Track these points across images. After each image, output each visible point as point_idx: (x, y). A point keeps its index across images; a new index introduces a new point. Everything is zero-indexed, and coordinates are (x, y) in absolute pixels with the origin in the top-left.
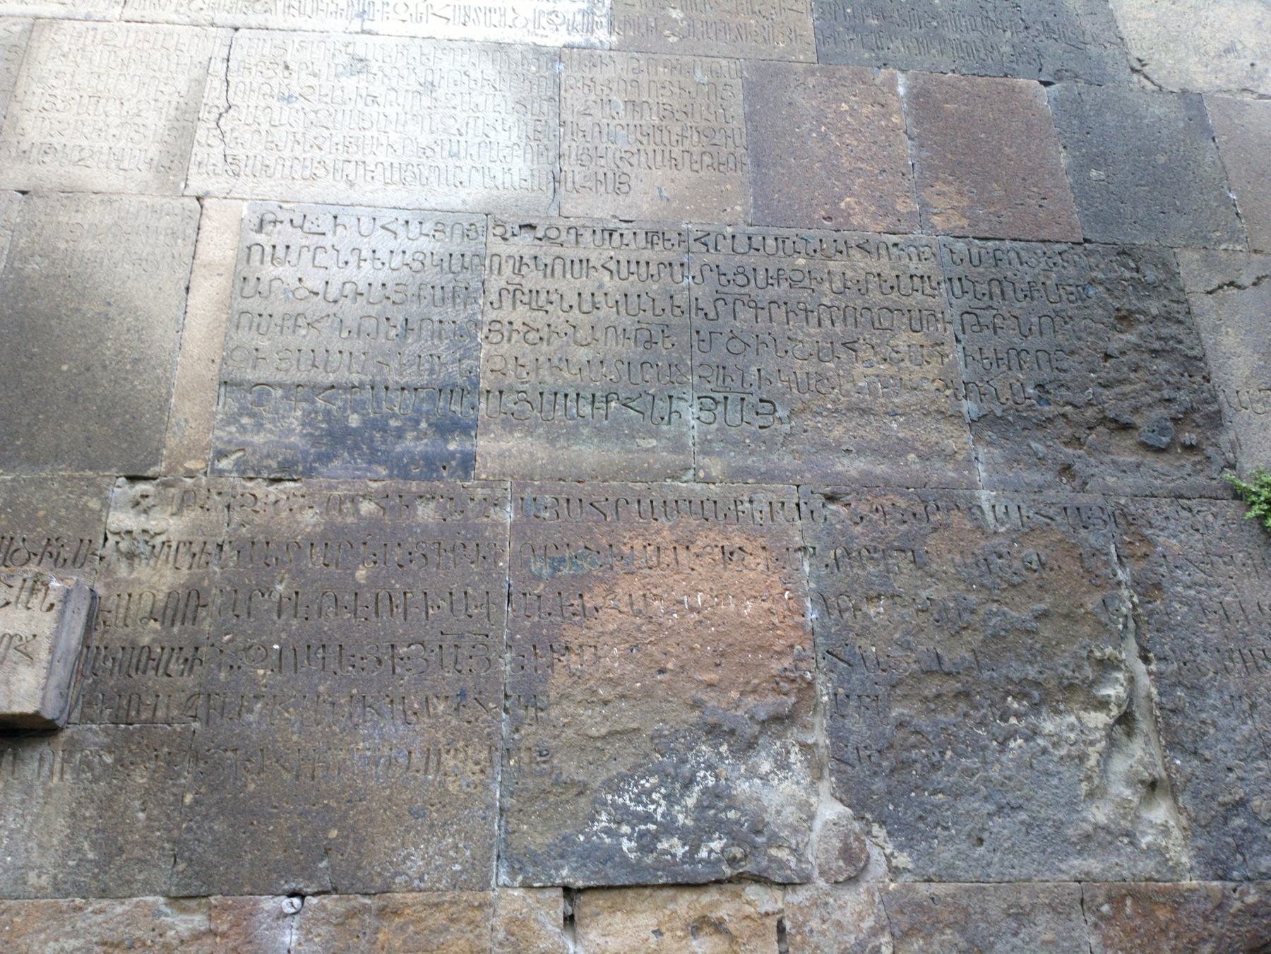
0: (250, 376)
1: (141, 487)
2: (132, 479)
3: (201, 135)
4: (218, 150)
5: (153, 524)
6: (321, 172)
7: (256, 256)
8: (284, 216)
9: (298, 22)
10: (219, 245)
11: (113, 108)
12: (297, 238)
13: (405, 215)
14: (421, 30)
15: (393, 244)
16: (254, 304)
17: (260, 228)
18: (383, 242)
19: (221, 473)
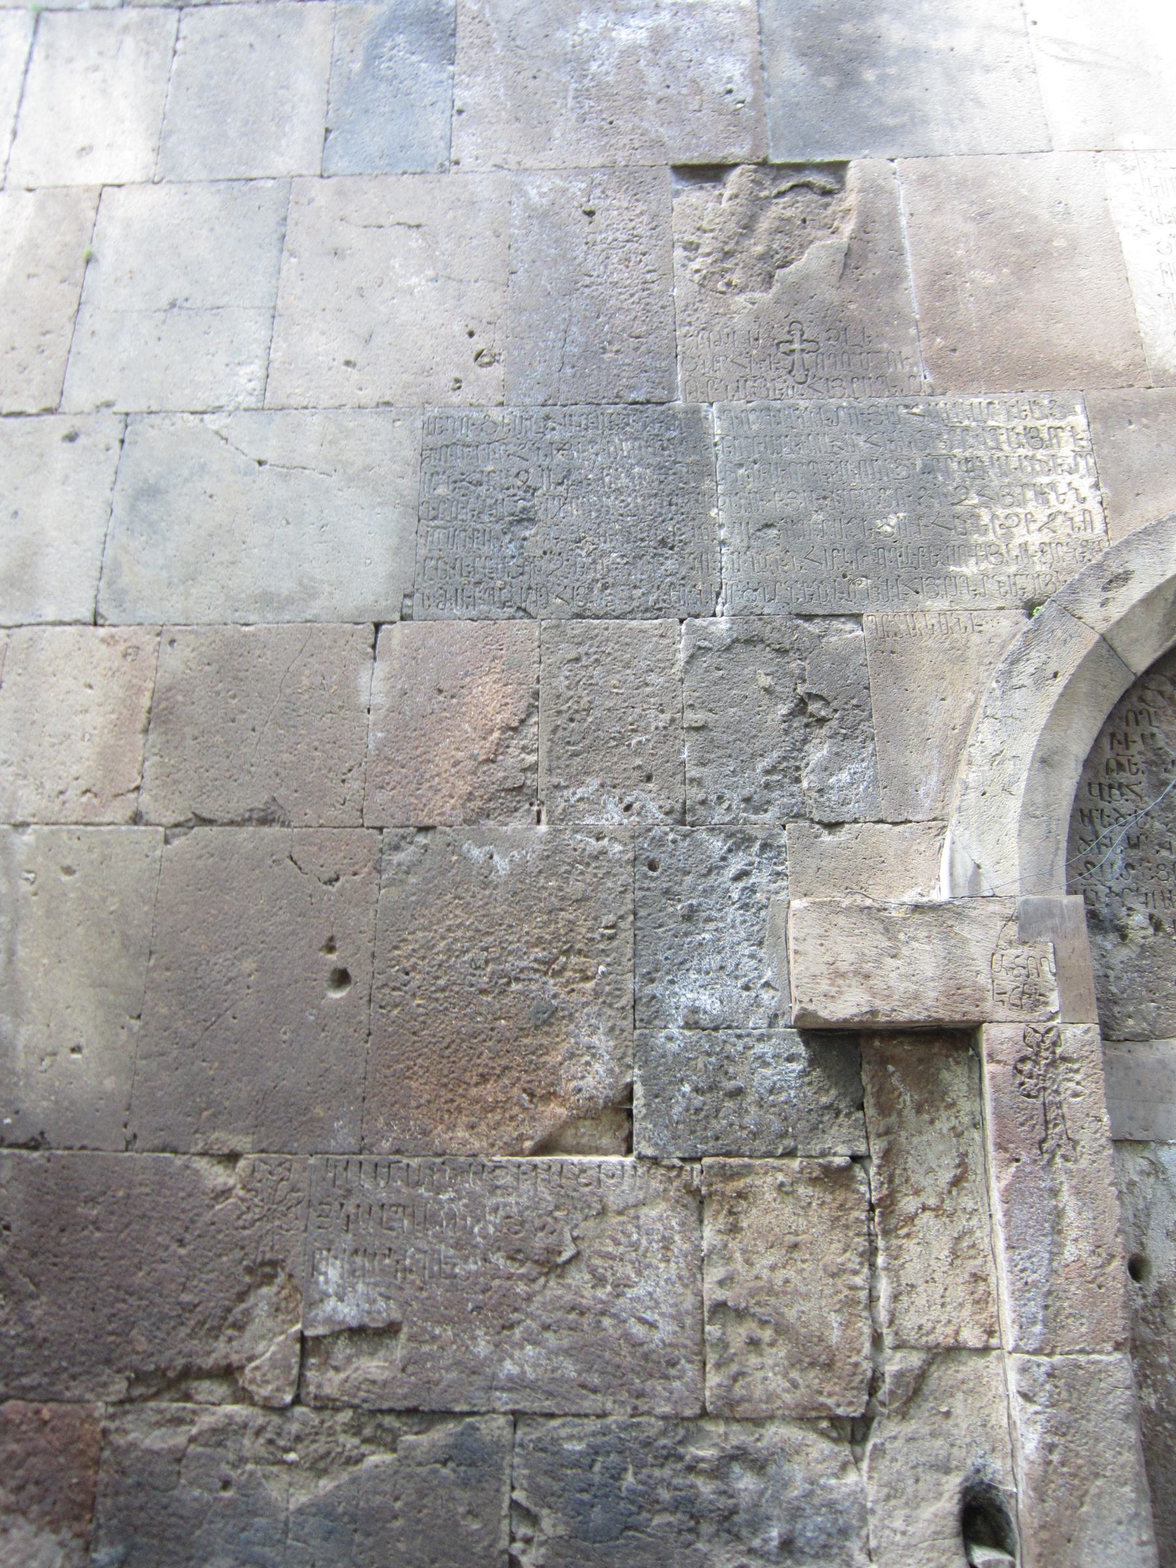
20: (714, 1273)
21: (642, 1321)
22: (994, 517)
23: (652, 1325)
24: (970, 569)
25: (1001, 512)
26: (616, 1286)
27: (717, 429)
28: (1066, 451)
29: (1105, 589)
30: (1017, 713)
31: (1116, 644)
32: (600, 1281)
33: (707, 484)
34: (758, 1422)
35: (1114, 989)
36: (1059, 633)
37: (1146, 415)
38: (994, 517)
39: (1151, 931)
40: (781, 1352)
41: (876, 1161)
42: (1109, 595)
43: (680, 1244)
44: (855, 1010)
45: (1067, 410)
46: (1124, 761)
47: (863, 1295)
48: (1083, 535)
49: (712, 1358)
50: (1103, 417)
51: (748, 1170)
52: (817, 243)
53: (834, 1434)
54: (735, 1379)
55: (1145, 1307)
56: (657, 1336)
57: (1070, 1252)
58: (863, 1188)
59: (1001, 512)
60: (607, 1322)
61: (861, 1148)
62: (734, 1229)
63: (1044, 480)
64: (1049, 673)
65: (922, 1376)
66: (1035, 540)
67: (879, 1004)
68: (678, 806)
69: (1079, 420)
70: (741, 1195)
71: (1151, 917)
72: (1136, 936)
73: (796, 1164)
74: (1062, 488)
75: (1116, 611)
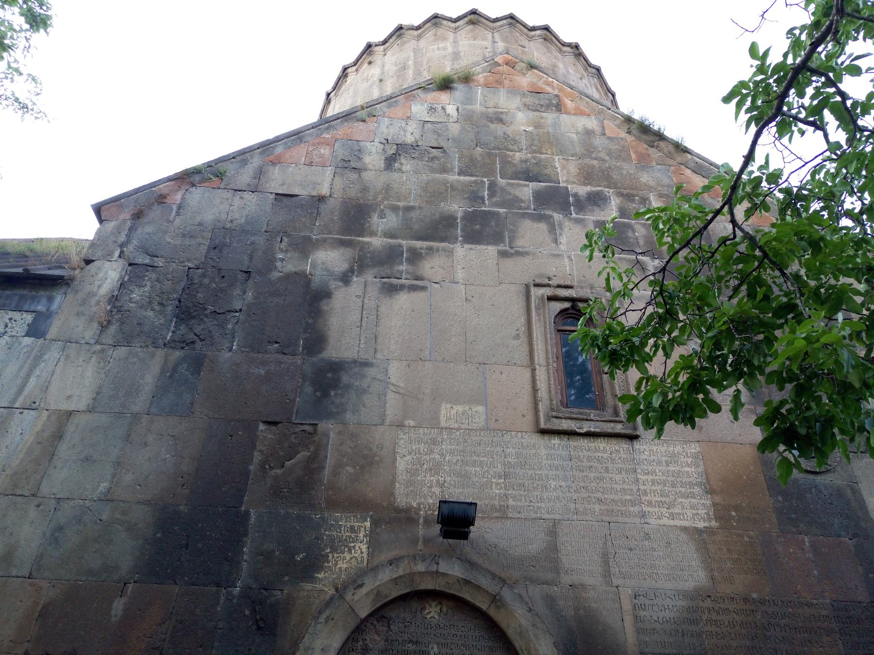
3: (611, 563)
4: (617, 569)
8: (641, 593)
9: (626, 520)
10: (627, 606)
11: (585, 553)
13: (673, 592)
14: (662, 522)
15: (673, 603)
18: (668, 602)
22: (333, 557)
24: (321, 576)
25: (336, 555)
27: (253, 520)
28: (361, 535)
31: (355, 608)
33: (245, 539)
37: (389, 523)
38: (333, 557)
45: (365, 520)
48: (360, 565)
50: (375, 523)
52: (302, 453)
59: (336, 555)
63: (352, 545)
66: (344, 566)
69: (368, 524)
74: (357, 548)
75: (356, 597)
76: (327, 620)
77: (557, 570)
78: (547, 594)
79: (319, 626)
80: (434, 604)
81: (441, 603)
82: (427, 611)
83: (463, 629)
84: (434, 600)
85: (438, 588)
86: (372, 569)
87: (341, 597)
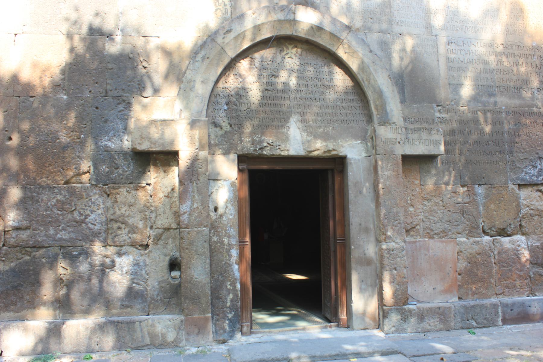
0: (453, 82)
1: (440, 108)
2: (438, 106)
5: (443, 116)
6: (458, 29)
7: (449, 52)
8: (453, 41)
12: (457, 48)
16: (451, 64)
17: (449, 45)
19: (453, 105)
20: (111, 212)
21: (92, 224)
23: (95, 225)
26: (86, 216)
29: (224, 34)
30: (196, 68)
32: (82, 215)
34: (121, 246)
35: (217, 142)
36: (210, 46)
39: (229, 126)
40: (127, 230)
41: (153, 185)
42: (225, 36)
43: (102, 206)
44: (146, 147)
46: (227, 81)
47: (148, 217)
49: (110, 232)
51: (119, 187)
53: (140, 248)
54: (115, 236)
55: (216, 219)
56: (96, 227)
57: (195, 205)
58: (149, 191)
60: (83, 225)
61: (149, 182)
62: (116, 202)
64: (206, 57)
65: (161, 235)
67: (152, 145)
68: (104, 91)
70: (118, 194)
71: (229, 124)
72: (224, 128)
73: (132, 186)
76: (203, 58)
77: (390, 22)
78: (382, 41)
79: (197, 64)
80: (290, 47)
81: (296, 47)
82: (285, 52)
83: (315, 66)
84: (290, 44)
85: (294, 34)
86: (238, 18)
87: (213, 40)
